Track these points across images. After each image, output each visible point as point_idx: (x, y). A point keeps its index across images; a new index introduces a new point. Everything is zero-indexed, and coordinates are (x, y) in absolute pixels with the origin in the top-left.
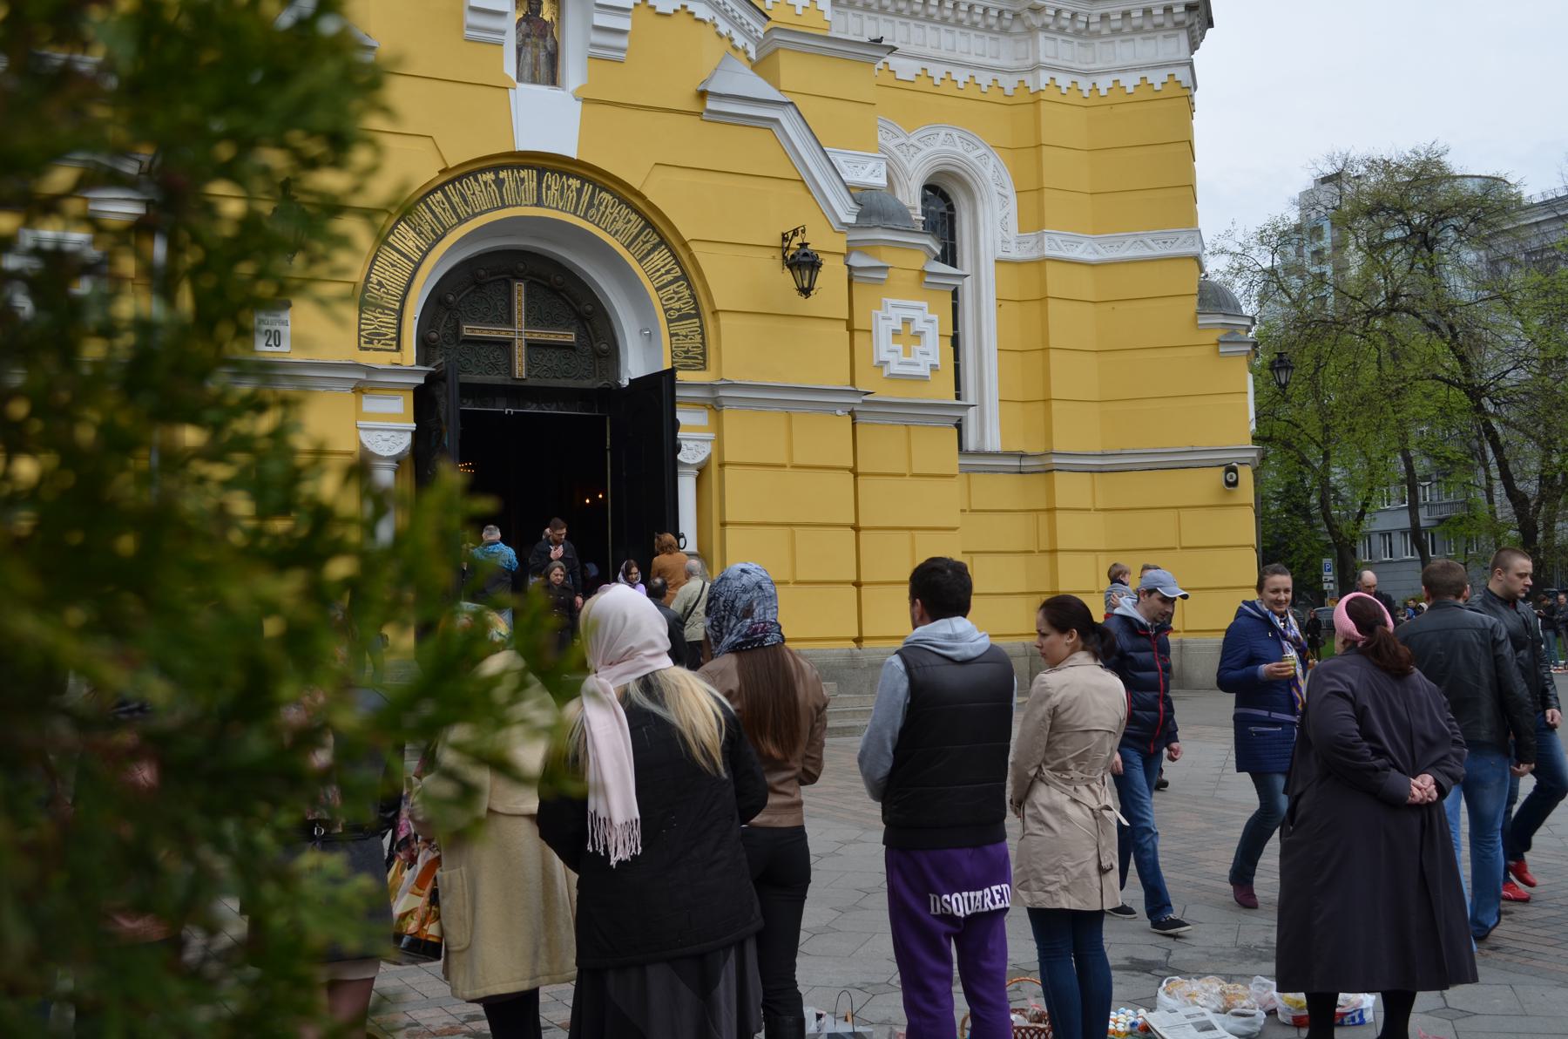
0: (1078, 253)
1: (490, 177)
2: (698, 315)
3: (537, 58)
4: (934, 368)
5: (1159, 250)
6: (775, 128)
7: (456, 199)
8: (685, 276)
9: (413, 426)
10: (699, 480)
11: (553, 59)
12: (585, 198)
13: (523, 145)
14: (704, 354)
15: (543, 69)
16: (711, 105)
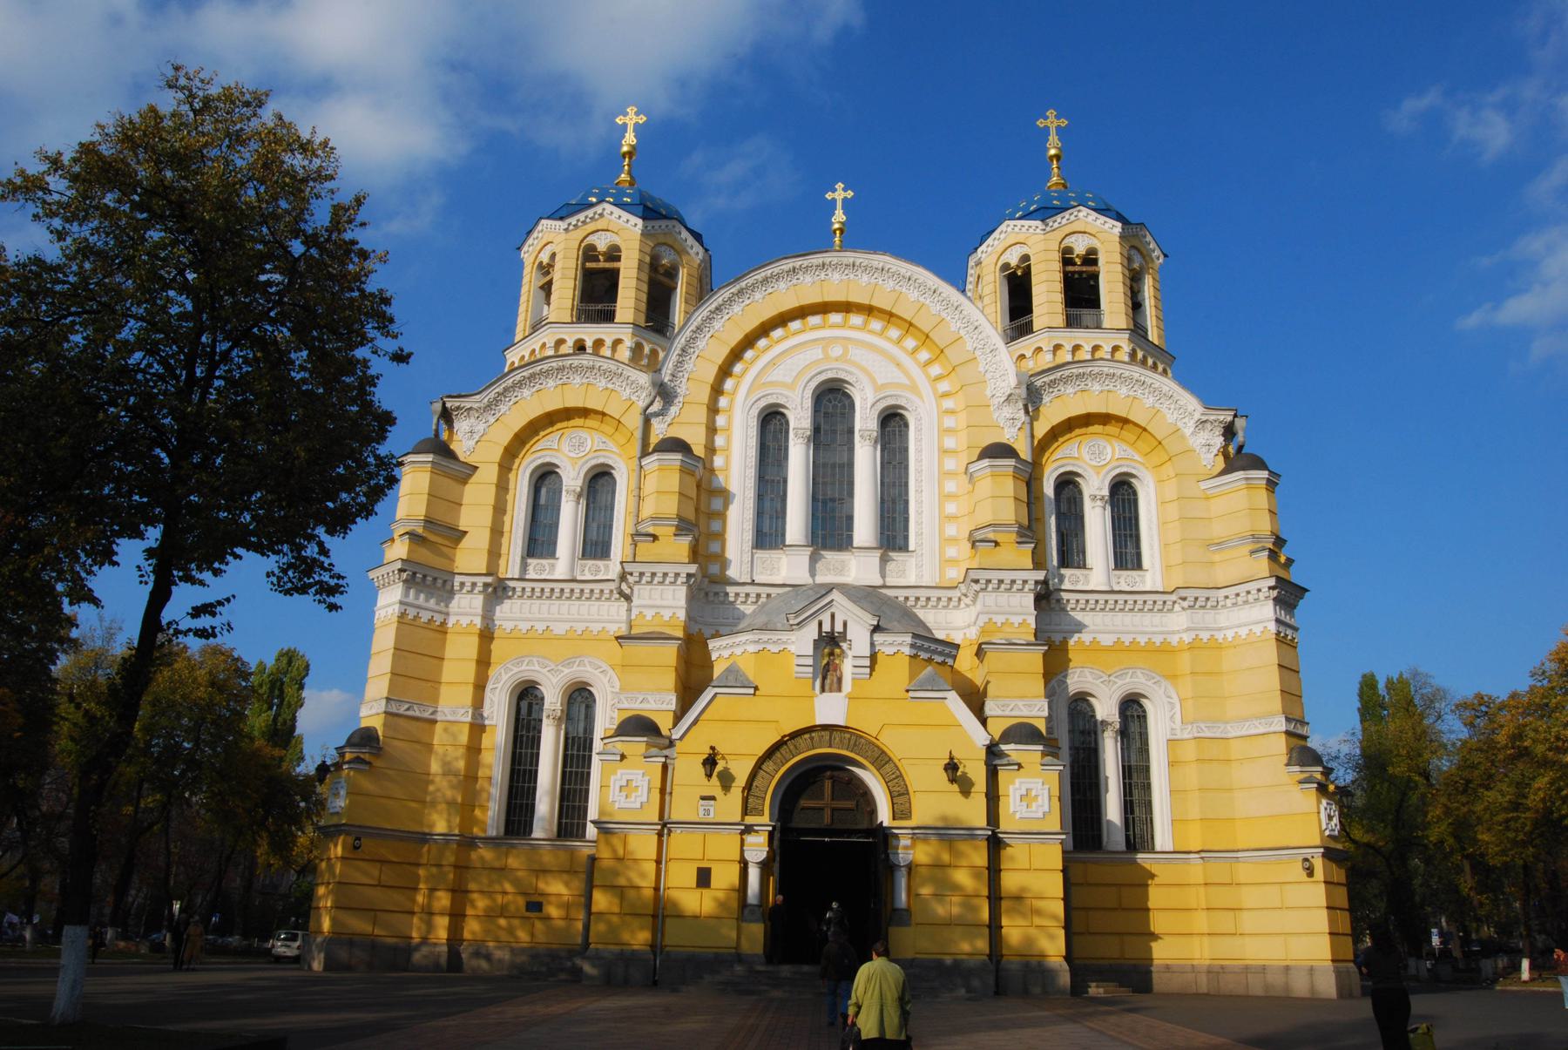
0: (1218, 735)
1: (807, 736)
2: (908, 794)
3: (833, 681)
4: (1044, 814)
5: (1262, 730)
6: (946, 701)
7: (792, 747)
8: (901, 775)
9: (767, 849)
10: (909, 873)
11: (840, 680)
12: (852, 742)
13: (820, 720)
14: (910, 812)
15: (835, 685)
16: (911, 694)
